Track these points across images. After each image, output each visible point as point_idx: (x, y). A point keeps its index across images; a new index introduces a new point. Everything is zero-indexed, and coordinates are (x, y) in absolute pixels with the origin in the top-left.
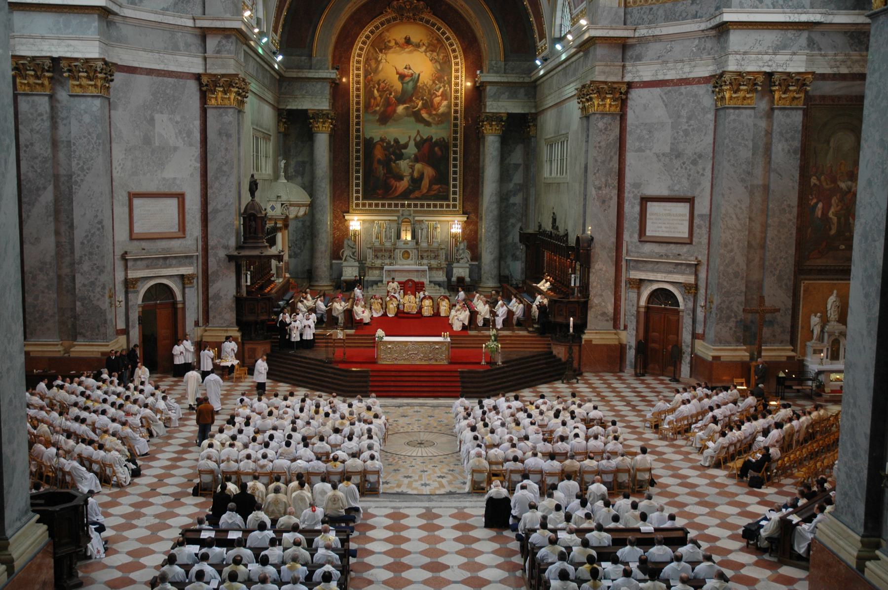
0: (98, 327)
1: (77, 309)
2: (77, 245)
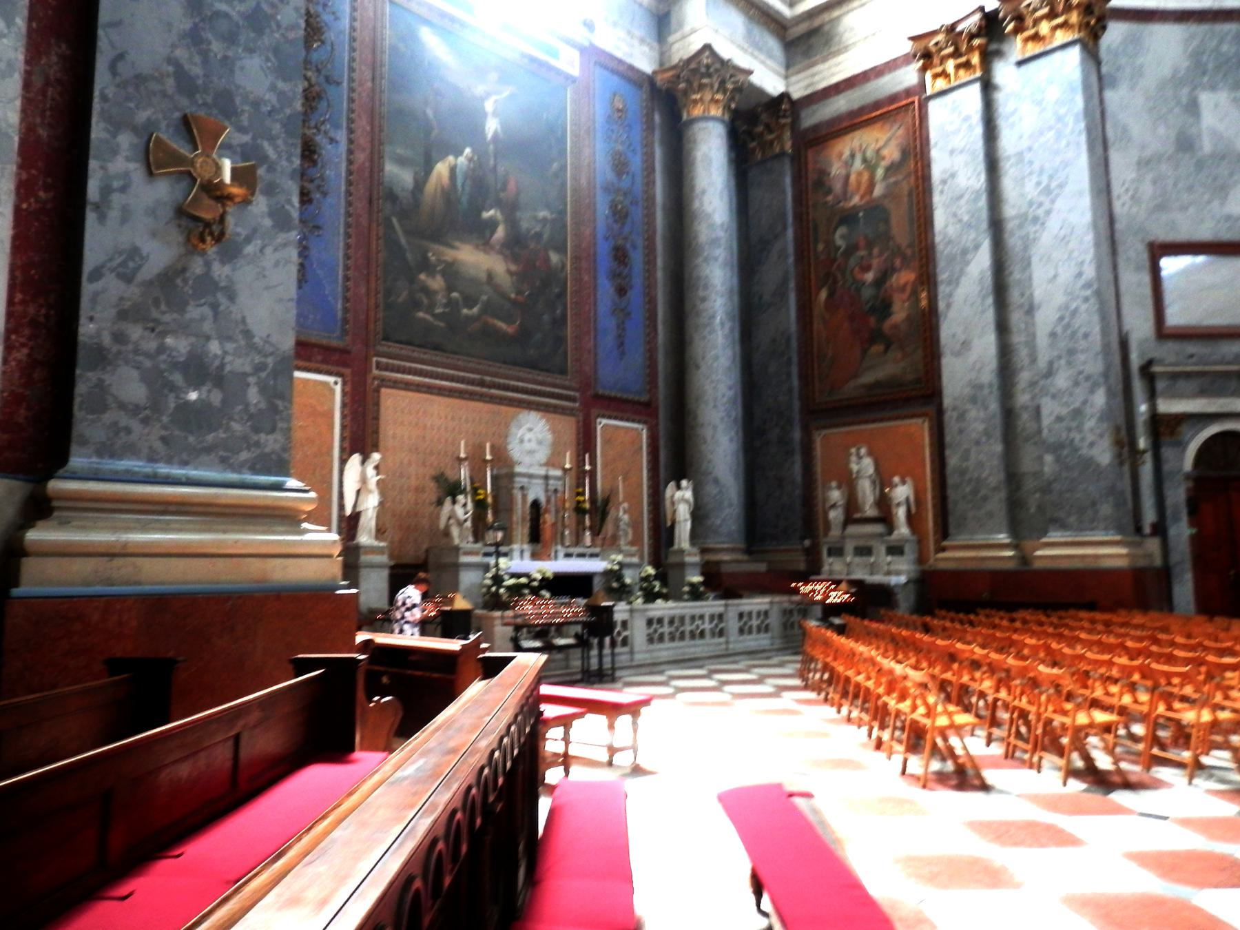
0: (1094, 504)
1: (1046, 469)
2: (1042, 341)
